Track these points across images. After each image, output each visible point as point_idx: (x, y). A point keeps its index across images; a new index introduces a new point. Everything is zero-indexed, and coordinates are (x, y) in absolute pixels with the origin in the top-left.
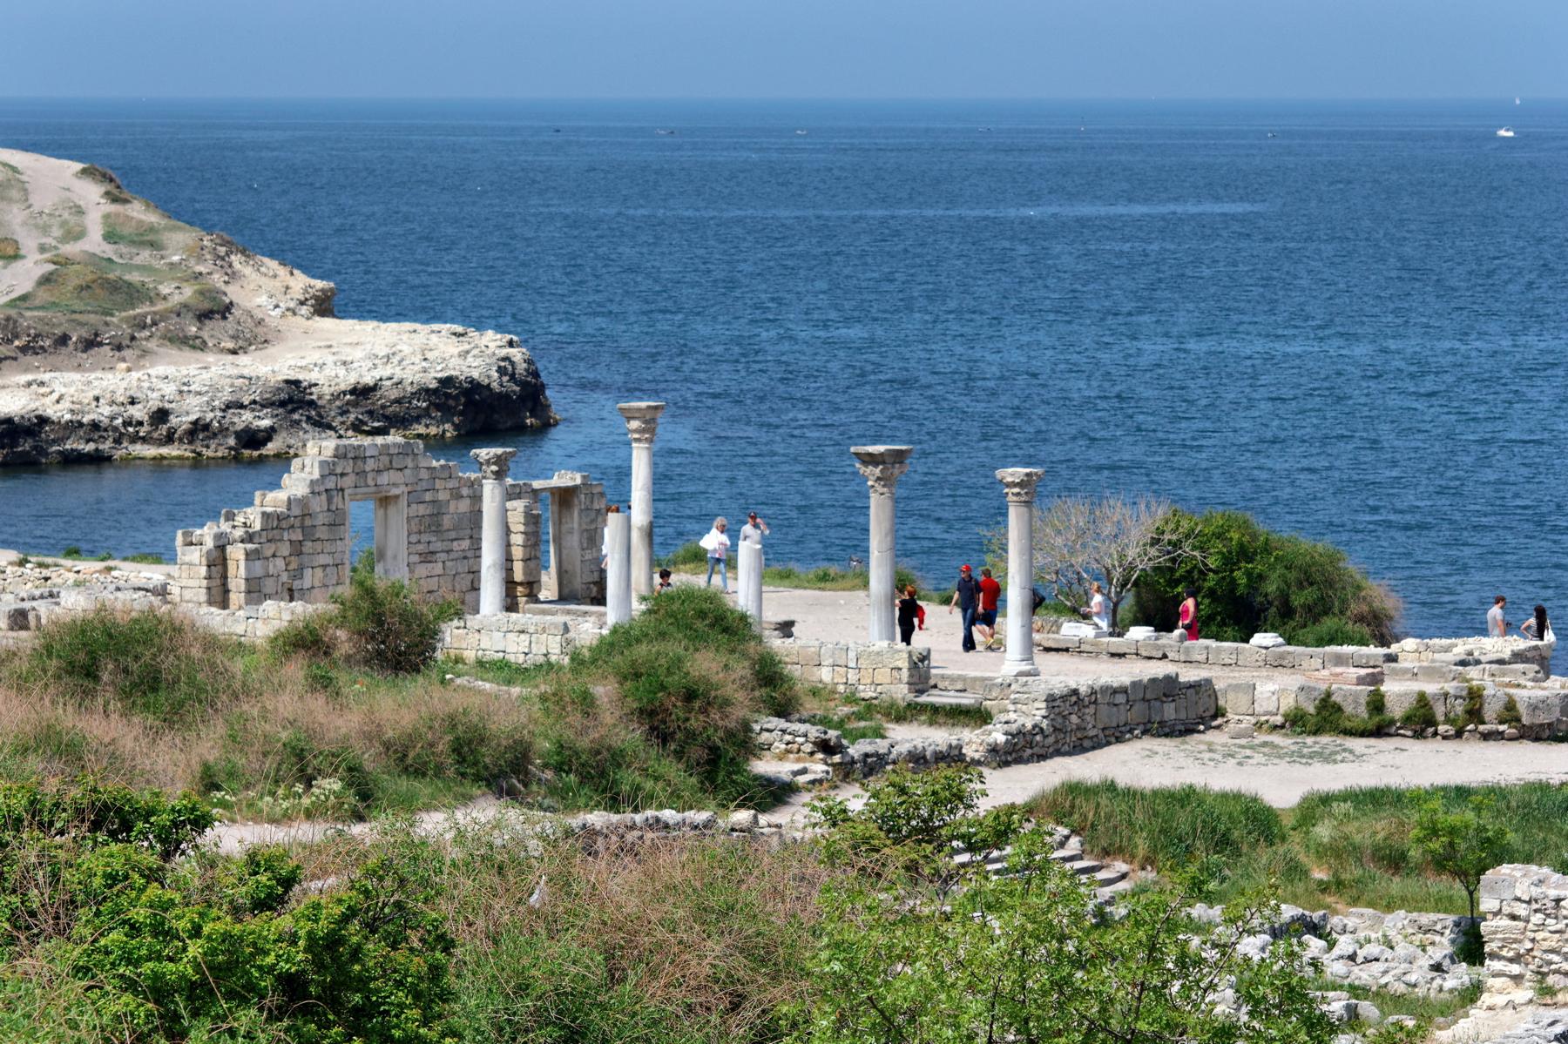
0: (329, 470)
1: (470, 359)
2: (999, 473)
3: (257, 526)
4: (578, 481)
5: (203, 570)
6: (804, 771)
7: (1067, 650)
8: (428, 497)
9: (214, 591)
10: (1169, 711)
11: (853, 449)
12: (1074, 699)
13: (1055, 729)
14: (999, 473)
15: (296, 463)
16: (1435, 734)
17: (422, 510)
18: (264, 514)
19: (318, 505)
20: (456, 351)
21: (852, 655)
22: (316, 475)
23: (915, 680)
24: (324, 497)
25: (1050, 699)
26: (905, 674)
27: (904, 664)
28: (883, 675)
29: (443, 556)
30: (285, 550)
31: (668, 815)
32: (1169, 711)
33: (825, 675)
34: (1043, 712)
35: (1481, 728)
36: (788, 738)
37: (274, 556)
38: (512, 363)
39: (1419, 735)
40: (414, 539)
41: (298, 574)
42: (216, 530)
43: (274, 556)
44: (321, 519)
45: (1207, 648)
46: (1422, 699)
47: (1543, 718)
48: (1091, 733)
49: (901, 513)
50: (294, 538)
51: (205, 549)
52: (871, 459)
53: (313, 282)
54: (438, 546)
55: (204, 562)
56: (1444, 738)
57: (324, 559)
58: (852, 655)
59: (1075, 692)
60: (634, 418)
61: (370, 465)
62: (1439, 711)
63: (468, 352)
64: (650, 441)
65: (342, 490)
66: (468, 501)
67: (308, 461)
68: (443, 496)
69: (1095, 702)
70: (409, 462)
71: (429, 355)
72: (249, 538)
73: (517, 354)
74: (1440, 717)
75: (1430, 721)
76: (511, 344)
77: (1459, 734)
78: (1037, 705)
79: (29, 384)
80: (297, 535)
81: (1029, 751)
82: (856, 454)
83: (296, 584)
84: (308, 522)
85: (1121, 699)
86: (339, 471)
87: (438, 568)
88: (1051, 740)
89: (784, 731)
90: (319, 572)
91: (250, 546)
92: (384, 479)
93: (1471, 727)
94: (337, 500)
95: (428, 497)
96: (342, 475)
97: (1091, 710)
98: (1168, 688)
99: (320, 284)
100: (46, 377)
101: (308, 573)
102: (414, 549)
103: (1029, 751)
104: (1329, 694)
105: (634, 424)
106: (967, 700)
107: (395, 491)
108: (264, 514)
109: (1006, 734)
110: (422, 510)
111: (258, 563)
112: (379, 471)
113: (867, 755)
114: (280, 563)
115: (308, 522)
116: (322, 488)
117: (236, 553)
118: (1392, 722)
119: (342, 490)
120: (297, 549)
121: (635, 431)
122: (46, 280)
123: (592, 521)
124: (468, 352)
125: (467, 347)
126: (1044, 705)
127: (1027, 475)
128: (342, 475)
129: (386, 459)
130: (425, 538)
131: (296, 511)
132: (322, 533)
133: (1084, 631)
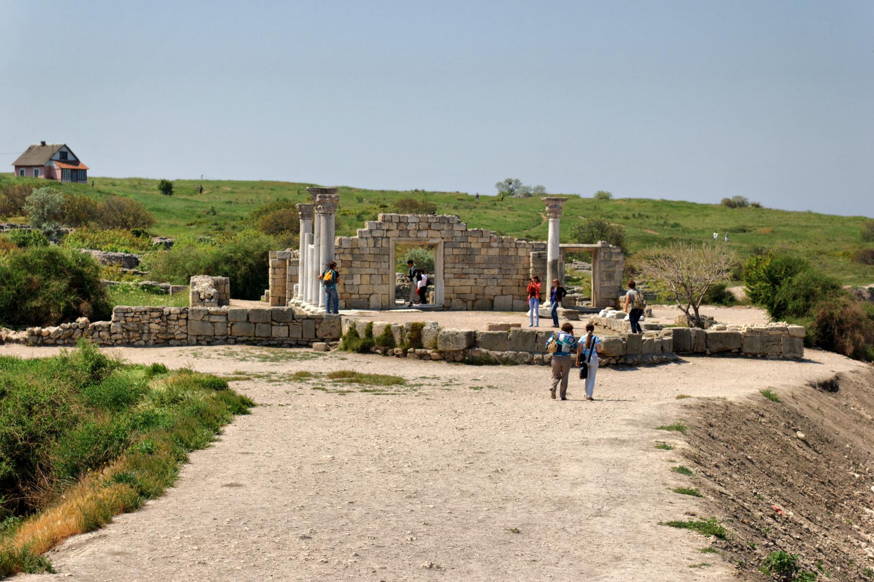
10: (280, 331)
16: (394, 354)
32: (280, 331)
35: (418, 350)
39: (385, 354)
46: (388, 327)
47: (452, 347)
50: (344, 258)
56: (398, 356)
62: (397, 337)
64: (556, 217)
66: (498, 250)
69: (187, 319)
74: (398, 342)
75: (392, 345)
77: (405, 354)
93: (411, 349)
95: (462, 245)
96: (387, 230)
97: (182, 322)
104: (355, 325)
112: (419, 230)
118: (372, 344)
123: (611, 266)
128: (387, 230)
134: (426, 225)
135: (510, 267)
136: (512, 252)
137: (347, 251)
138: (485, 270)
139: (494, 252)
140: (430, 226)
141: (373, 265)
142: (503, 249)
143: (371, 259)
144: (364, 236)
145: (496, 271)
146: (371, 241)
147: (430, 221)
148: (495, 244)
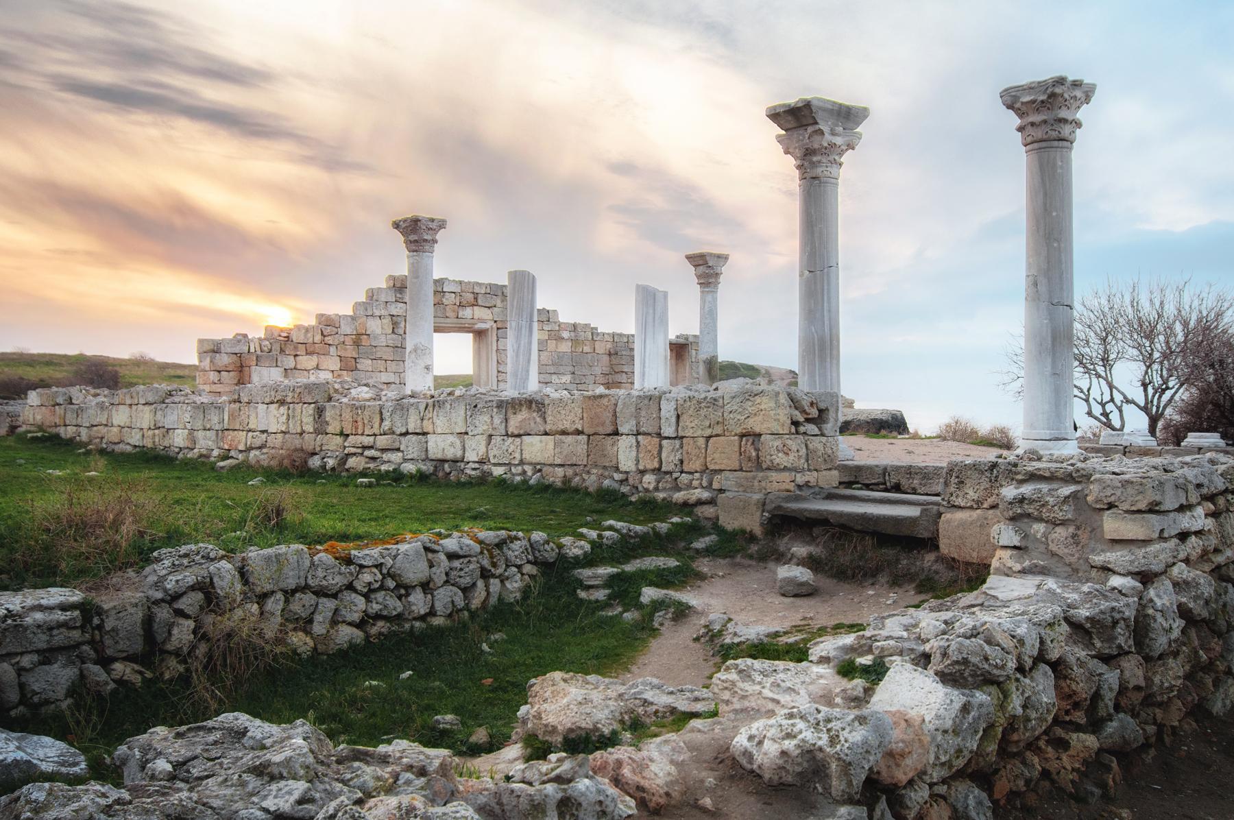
30: (334, 364)
37: (317, 368)
43: (317, 368)
80: (350, 352)
131: (346, 329)
134: (470, 297)
135: (585, 371)
136: (587, 349)
137: (348, 340)
138: (554, 377)
139: (565, 347)
140: (476, 299)
141: (392, 366)
142: (575, 341)
143: (388, 354)
144: (377, 313)
145: (567, 379)
146: (387, 321)
147: (477, 290)
148: (566, 335)
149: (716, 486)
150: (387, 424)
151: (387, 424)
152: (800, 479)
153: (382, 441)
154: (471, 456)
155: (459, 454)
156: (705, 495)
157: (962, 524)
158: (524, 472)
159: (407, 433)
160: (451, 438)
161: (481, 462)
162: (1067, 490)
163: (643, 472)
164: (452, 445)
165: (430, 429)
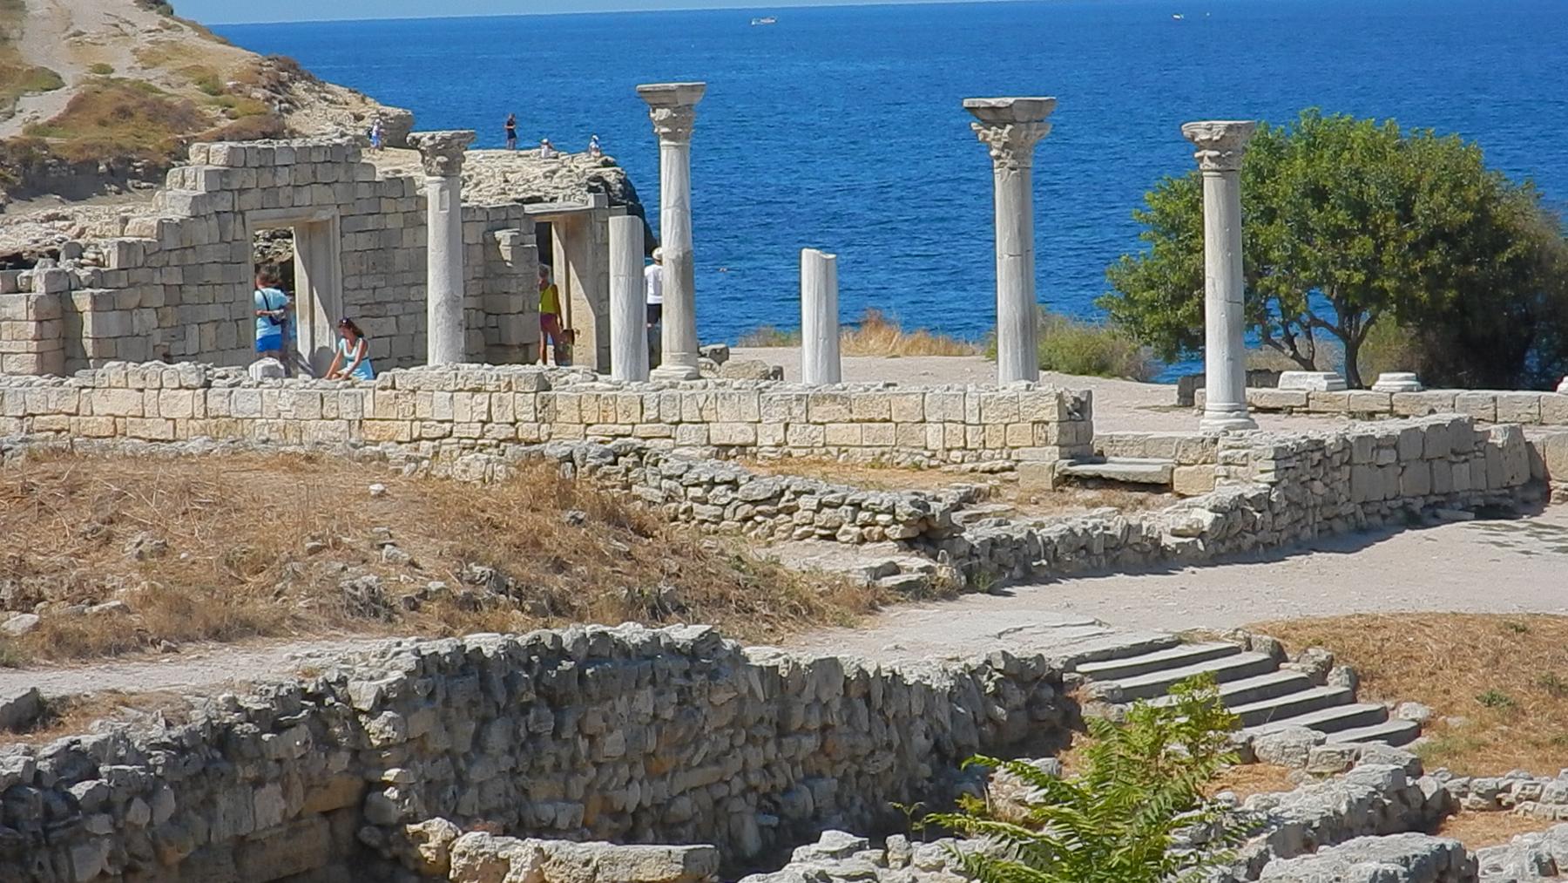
0: (220, 180)
1: (556, 179)
2: (1187, 129)
3: (114, 265)
4: (591, 204)
5: (32, 327)
6: (896, 570)
7: (1291, 411)
8: (371, 223)
9: (48, 357)
10: (1461, 478)
11: (966, 103)
12: (1317, 456)
13: (1291, 503)
14: (1187, 129)
15: (173, 175)
17: (363, 242)
18: (120, 244)
19: (206, 232)
20: (539, 172)
21: (971, 404)
22: (201, 191)
23: (1071, 438)
24: (214, 222)
25: (1282, 456)
26: (1054, 430)
27: (1051, 414)
28: (1020, 434)
29: (395, 308)
30: (158, 298)
31: (632, 632)
33: (933, 436)
34: (1271, 477)
36: (863, 516)
37: (140, 306)
38: (606, 184)
40: (352, 283)
41: (179, 332)
42: (50, 268)
43: (140, 306)
44: (211, 254)
45: (1494, 399)
48: (1346, 509)
49: (1040, 191)
51: (33, 296)
52: (996, 117)
53: (388, 109)
54: (388, 293)
55: (32, 316)
57: (214, 312)
58: (971, 404)
59: (1319, 445)
60: (662, 106)
61: (284, 177)
63: (554, 172)
65: (242, 213)
67: (189, 171)
68: (393, 223)
70: (340, 173)
71: (509, 176)
72: (99, 279)
73: (610, 175)
76: (606, 164)
78: (1261, 465)
79: (49, 218)
81: (1251, 538)
82: (972, 110)
83: (176, 348)
84: (191, 258)
85: (1388, 457)
86: (236, 185)
87: (389, 326)
88: (1284, 520)
89: (858, 506)
90: (209, 330)
91: (97, 291)
92: (305, 197)
94: (235, 228)
95: (371, 223)
96: (241, 191)
98: (1461, 441)
99: (393, 111)
100: (67, 210)
101: (193, 331)
102: (352, 297)
103: (1251, 538)
105: (662, 114)
106: (1151, 468)
107: (323, 215)
108: (120, 244)
109: (1214, 510)
110: (363, 242)
111: (113, 316)
113: (994, 543)
114: (150, 317)
115: (191, 258)
116: (210, 210)
117: (82, 300)
119: (242, 213)
120: (175, 296)
121: (663, 123)
122: (77, 106)
124: (554, 172)
125: (554, 166)
126: (1272, 465)
127: (1229, 128)
128: (241, 191)
129: (308, 169)
130: (368, 282)
132: (213, 274)
133: (1316, 381)
147: (315, 157)
149: (1014, 457)
150: (651, 413)
151: (651, 413)
152: (1074, 451)
153: (642, 430)
154: (766, 441)
155: (751, 439)
156: (1007, 464)
157: (1187, 473)
158: (828, 452)
159: (681, 422)
160: (742, 426)
161: (778, 446)
162: (1243, 452)
163: (949, 450)
164: (742, 432)
165: (714, 418)
